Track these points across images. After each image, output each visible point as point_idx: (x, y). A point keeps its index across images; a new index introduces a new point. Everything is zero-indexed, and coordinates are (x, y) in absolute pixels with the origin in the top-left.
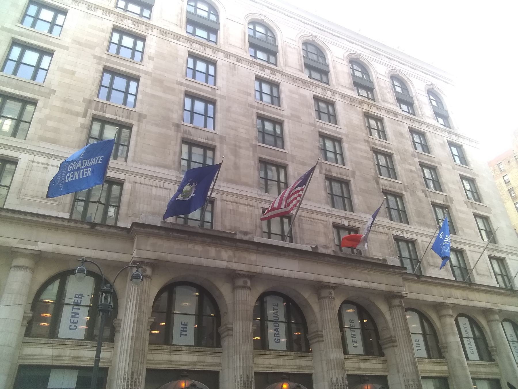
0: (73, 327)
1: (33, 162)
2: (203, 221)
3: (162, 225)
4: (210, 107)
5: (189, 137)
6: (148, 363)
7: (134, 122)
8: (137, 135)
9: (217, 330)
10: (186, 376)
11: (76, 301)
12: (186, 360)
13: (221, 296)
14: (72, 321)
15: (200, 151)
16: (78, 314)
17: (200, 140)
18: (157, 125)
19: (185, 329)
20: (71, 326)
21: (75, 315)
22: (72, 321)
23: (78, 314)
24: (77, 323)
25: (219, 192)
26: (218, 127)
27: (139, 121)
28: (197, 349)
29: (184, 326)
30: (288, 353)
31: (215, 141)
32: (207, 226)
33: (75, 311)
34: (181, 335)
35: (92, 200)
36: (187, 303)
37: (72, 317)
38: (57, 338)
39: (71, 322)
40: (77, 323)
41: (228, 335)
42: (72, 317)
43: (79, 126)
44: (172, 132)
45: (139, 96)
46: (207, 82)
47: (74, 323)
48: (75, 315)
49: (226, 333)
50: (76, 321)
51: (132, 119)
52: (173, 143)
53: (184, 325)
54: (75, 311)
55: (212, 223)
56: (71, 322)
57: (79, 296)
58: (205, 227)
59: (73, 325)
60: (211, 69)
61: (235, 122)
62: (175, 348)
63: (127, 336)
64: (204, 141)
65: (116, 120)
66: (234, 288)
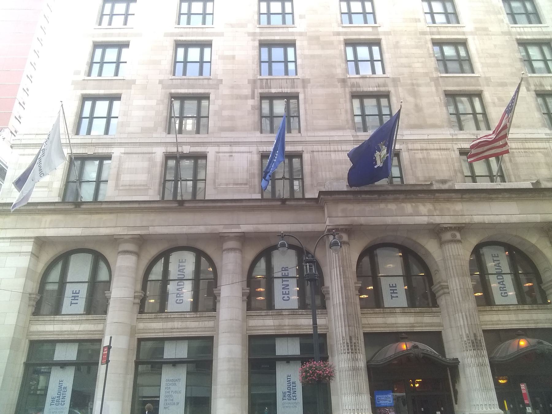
0: (286, 298)
1: (219, 153)
4: (375, 49)
5: (358, 89)
6: (363, 327)
7: (299, 90)
8: (305, 103)
9: (431, 290)
10: (406, 338)
11: (284, 274)
12: (403, 321)
13: (428, 253)
14: (284, 293)
15: (373, 102)
16: (288, 285)
17: (371, 89)
18: (323, 86)
19: (395, 291)
22: (284, 293)
23: (288, 285)
24: (289, 294)
25: (404, 141)
26: (388, 69)
27: (304, 87)
28: (412, 310)
29: (393, 288)
30: (521, 307)
32: (397, 181)
33: (284, 283)
35: (277, 177)
36: (391, 265)
37: (283, 288)
40: (289, 294)
41: (444, 293)
42: (283, 288)
43: (250, 108)
44: (338, 90)
45: (299, 61)
46: (366, 22)
47: (286, 294)
49: (441, 292)
50: (287, 293)
51: (297, 87)
52: (342, 100)
54: (285, 283)
55: (401, 177)
57: (285, 269)
58: (394, 183)
59: (286, 296)
61: (406, 57)
62: (388, 310)
63: (338, 302)
64: (375, 89)
65: (282, 93)
66: (442, 243)
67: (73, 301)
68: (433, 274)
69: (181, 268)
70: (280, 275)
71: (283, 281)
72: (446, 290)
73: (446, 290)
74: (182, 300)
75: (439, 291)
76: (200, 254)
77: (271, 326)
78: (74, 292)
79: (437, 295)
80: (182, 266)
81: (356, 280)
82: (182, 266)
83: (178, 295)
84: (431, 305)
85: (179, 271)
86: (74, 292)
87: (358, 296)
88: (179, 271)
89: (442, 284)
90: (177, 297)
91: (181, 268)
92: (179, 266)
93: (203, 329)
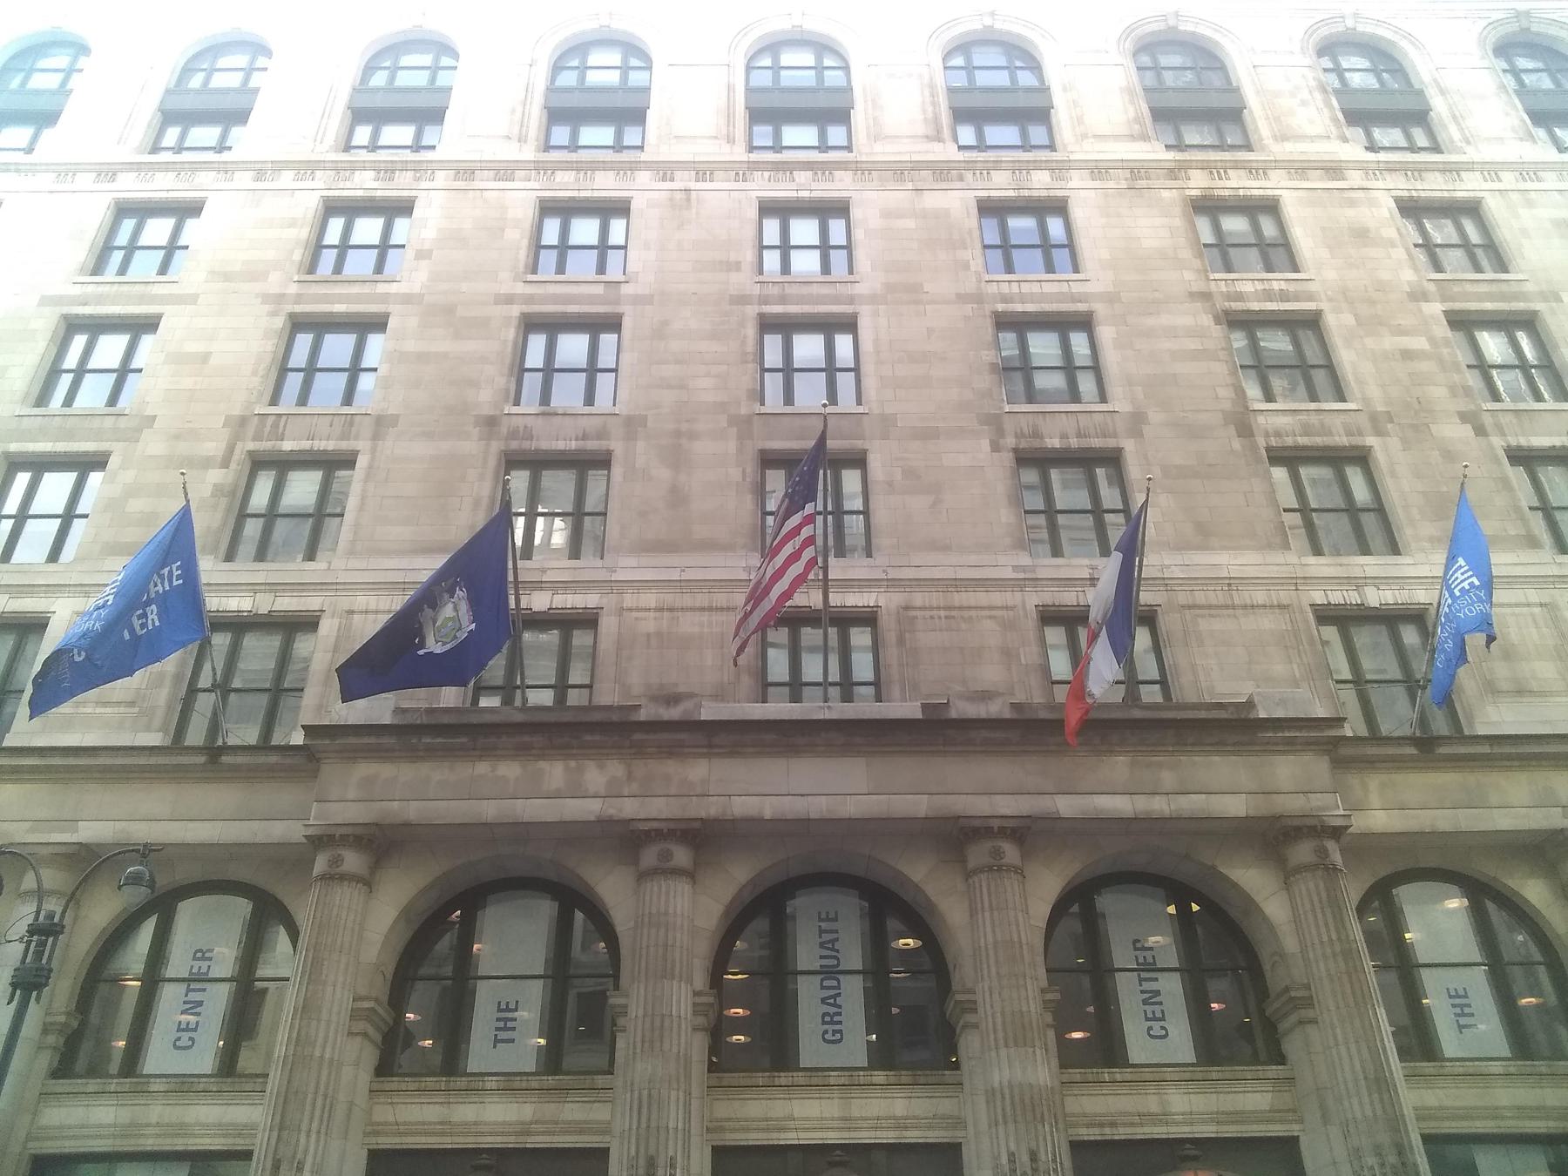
0: (1157, 1031)
2: (1131, 682)
3: (1015, 716)
4: (1079, 341)
9: (1262, 1011)
10: (1195, 1158)
12: (1189, 1108)
13: (1250, 906)
14: (1150, 1015)
15: (1324, 472)
20: (1150, 1028)
21: (1152, 998)
22: (1150, 1015)
23: (1158, 993)
24: (1163, 1019)
25: (1165, 583)
26: (1115, 389)
31: (1115, 436)
32: (1150, 694)
33: (1147, 986)
37: (1145, 1002)
40: (1163, 1019)
42: (1145, 1002)
45: (868, 368)
46: (1050, 268)
47: (1155, 1019)
49: (1293, 1018)
50: (1159, 1015)
54: (1147, 986)
55: (1163, 682)
56: (1147, 1019)
59: (1156, 1025)
60: (1055, 226)
62: (1147, 1074)
66: (1288, 875)
67: (503, 1035)
68: (1267, 967)
69: (826, 937)
70: (816, 966)
71: (1141, 980)
72: (1310, 1013)
73: (1310, 1013)
74: (840, 1031)
75: (1286, 1015)
77: (813, 1119)
79: (1284, 1026)
80: (826, 931)
81: (1044, 983)
82: (826, 931)
83: (827, 1019)
87: (1051, 1034)
88: (822, 945)
89: (1293, 994)
90: (824, 1023)
91: (826, 937)
92: (821, 931)
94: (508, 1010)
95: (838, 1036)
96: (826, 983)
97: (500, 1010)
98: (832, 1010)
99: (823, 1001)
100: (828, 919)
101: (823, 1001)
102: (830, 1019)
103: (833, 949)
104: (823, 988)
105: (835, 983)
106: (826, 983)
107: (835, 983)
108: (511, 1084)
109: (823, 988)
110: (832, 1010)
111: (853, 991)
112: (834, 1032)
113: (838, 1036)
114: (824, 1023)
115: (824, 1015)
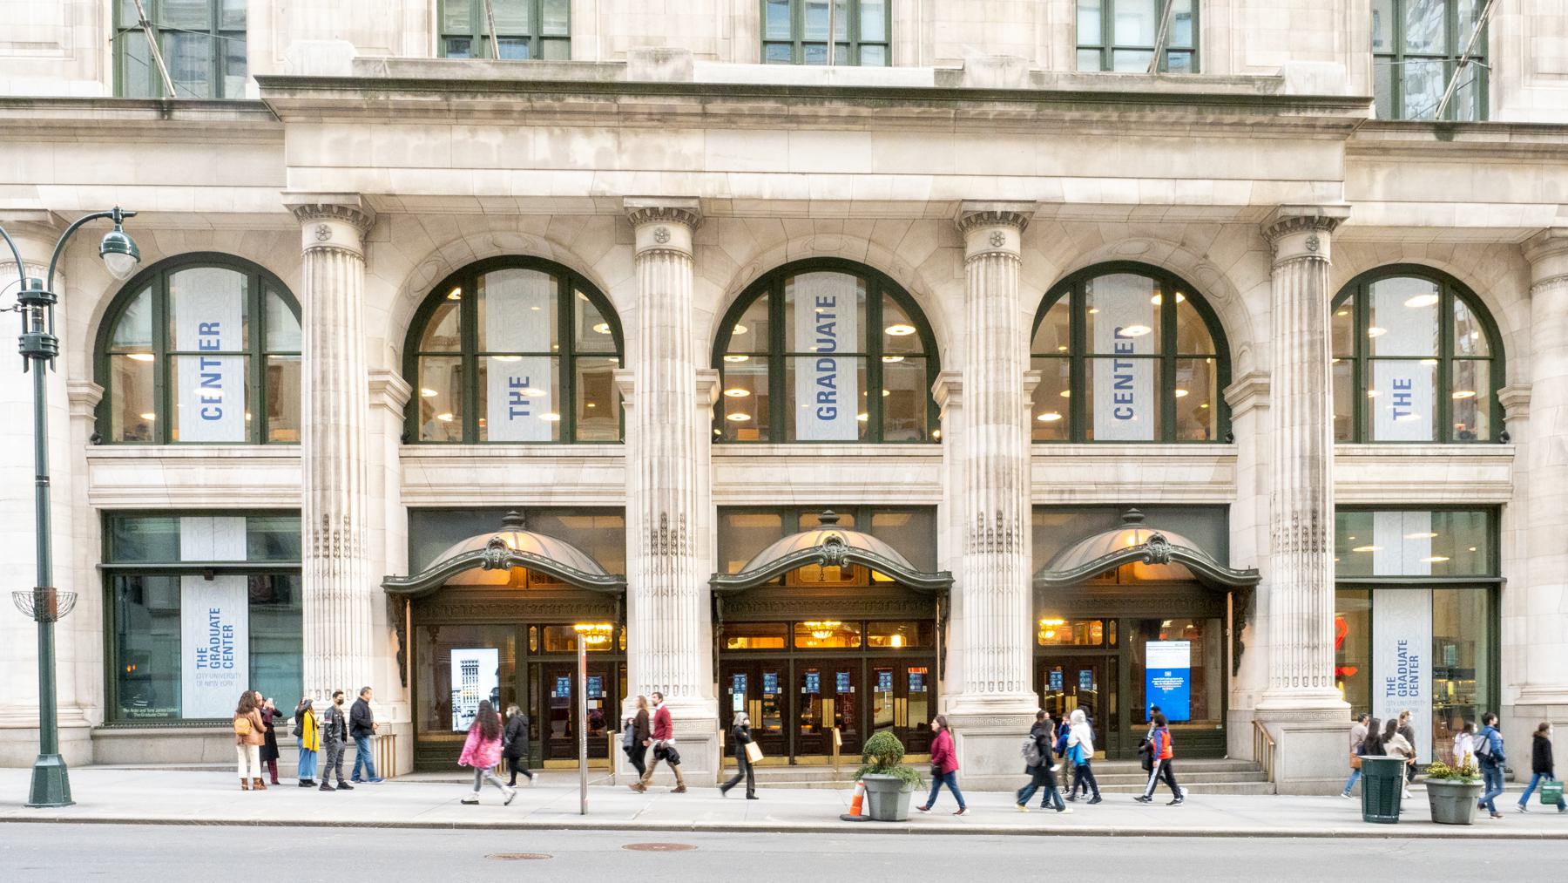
16: (1130, 378)
19: (1406, 400)
21: (1123, 382)
23: (1130, 378)
24: (1131, 401)
28: (1170, 449)
29: (1402, 392)
34: (1396, 414)
37: (1117, 386)
38: (1093, 441)
39: (1117, 401)
40: (1131, 401)
42: (1117, 386)
48: (1123, 382)
53: (1402, 387)
54: (1121, 371)
56: (1117, 401)
59: (1124, 407)
69: (823, 322)
70: (814, 349)
74: (834, 409)
75: (1242, 401)
76: (1450, 287)
78: (515, 381)
79: (1236, 411)
81: (1027, 367)
84: (1214, 436)
85: (819, 329)
86: (515, 381)
87: (1028, 414)
88: (819, 329)
91: (823, 322)
93: (1477, 487)
94: (519, 385)
95: (832, 413)
96: (823, 365)
97: (512, 385)
98: (827, 390)
99: (820, 381)
100: (826, 304)
101: (820, 381)
102: (824, 398)
103: (830, 333)
104: (819, 369)
105: (830, 365)
106: (823, 365)
107: (830, 365)
108: (529, 449)
109: (819, 369)
110: (827, 390)
111: (848, 374)
112: (829, 410)
113: (832, 413)
114: (819, 401)
115: (820, 394)
